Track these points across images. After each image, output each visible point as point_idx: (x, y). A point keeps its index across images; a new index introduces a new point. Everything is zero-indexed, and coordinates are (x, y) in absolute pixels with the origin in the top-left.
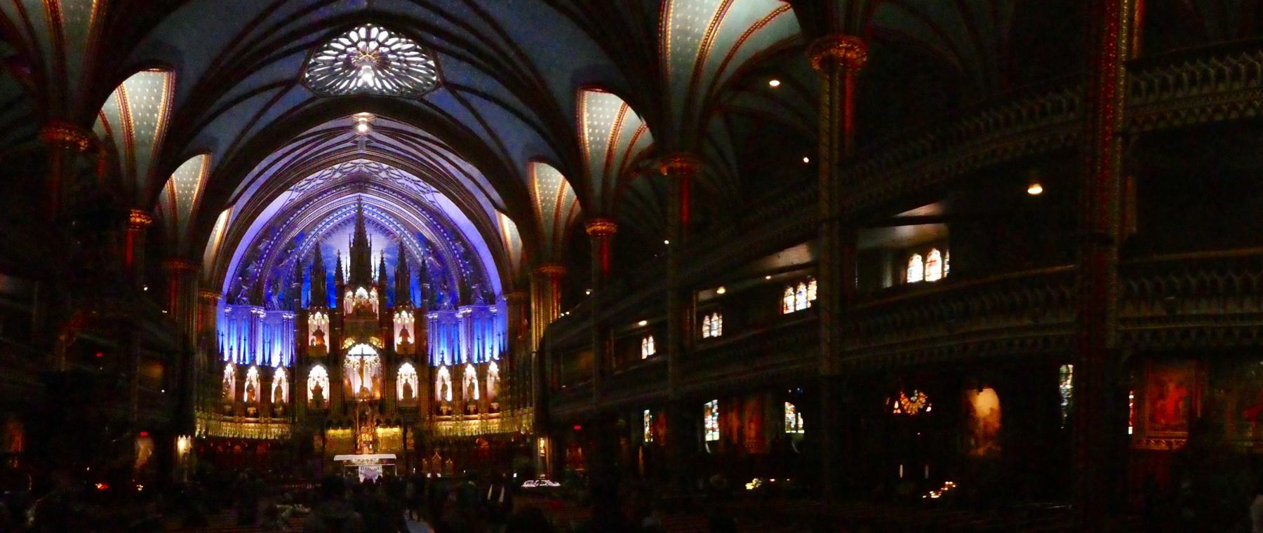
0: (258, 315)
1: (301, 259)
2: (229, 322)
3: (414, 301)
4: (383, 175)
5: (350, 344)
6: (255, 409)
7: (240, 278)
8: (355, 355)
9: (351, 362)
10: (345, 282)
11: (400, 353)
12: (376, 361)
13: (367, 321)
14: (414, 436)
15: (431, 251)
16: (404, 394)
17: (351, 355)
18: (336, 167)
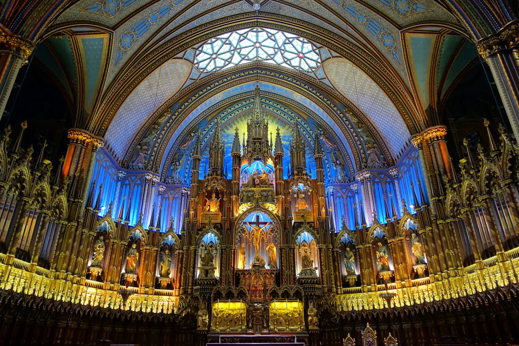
0: (153, 183)
1: (203, 143)
2: (122, 187)
3: (310, 172)
4: (279, 59)
5: (245, 210)
6: (135, 276)
7: (139, 147)
8: (250, 223)
9: (247, 232)
10: (242, 154)
11: (297, 221)
12: (272, 231)
13: (263, 189)
14: (316, 315)
15: (322, 133)
16: (304, 266)
17: (245, 223)
18: (234, 37)
